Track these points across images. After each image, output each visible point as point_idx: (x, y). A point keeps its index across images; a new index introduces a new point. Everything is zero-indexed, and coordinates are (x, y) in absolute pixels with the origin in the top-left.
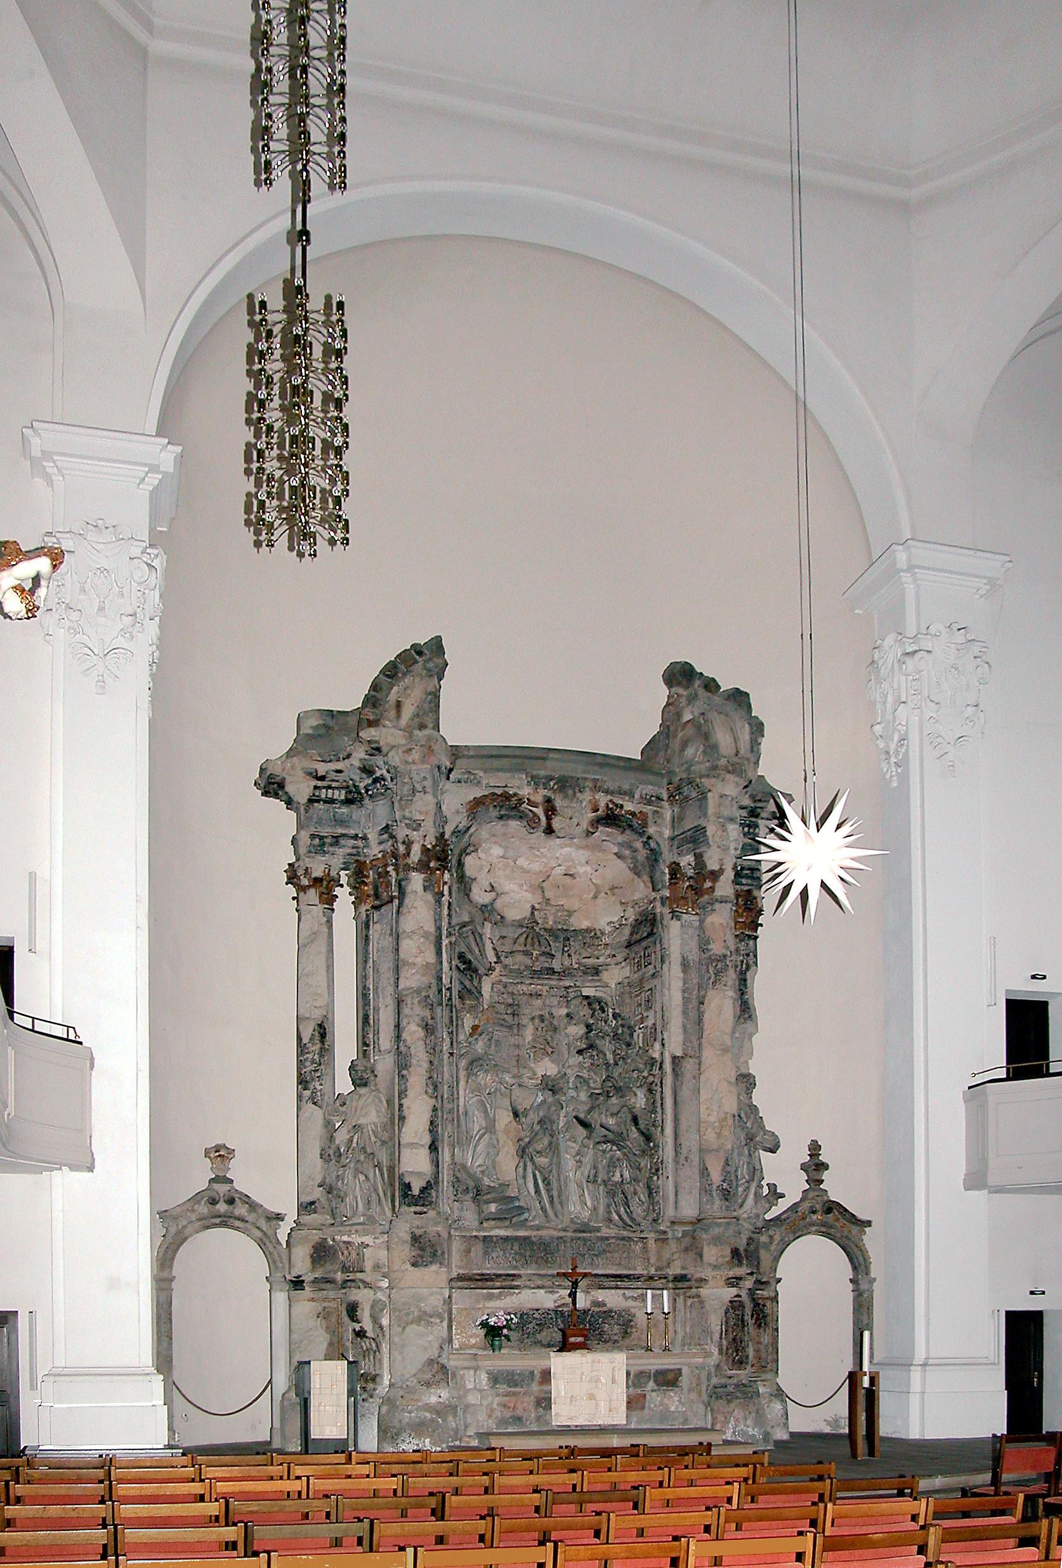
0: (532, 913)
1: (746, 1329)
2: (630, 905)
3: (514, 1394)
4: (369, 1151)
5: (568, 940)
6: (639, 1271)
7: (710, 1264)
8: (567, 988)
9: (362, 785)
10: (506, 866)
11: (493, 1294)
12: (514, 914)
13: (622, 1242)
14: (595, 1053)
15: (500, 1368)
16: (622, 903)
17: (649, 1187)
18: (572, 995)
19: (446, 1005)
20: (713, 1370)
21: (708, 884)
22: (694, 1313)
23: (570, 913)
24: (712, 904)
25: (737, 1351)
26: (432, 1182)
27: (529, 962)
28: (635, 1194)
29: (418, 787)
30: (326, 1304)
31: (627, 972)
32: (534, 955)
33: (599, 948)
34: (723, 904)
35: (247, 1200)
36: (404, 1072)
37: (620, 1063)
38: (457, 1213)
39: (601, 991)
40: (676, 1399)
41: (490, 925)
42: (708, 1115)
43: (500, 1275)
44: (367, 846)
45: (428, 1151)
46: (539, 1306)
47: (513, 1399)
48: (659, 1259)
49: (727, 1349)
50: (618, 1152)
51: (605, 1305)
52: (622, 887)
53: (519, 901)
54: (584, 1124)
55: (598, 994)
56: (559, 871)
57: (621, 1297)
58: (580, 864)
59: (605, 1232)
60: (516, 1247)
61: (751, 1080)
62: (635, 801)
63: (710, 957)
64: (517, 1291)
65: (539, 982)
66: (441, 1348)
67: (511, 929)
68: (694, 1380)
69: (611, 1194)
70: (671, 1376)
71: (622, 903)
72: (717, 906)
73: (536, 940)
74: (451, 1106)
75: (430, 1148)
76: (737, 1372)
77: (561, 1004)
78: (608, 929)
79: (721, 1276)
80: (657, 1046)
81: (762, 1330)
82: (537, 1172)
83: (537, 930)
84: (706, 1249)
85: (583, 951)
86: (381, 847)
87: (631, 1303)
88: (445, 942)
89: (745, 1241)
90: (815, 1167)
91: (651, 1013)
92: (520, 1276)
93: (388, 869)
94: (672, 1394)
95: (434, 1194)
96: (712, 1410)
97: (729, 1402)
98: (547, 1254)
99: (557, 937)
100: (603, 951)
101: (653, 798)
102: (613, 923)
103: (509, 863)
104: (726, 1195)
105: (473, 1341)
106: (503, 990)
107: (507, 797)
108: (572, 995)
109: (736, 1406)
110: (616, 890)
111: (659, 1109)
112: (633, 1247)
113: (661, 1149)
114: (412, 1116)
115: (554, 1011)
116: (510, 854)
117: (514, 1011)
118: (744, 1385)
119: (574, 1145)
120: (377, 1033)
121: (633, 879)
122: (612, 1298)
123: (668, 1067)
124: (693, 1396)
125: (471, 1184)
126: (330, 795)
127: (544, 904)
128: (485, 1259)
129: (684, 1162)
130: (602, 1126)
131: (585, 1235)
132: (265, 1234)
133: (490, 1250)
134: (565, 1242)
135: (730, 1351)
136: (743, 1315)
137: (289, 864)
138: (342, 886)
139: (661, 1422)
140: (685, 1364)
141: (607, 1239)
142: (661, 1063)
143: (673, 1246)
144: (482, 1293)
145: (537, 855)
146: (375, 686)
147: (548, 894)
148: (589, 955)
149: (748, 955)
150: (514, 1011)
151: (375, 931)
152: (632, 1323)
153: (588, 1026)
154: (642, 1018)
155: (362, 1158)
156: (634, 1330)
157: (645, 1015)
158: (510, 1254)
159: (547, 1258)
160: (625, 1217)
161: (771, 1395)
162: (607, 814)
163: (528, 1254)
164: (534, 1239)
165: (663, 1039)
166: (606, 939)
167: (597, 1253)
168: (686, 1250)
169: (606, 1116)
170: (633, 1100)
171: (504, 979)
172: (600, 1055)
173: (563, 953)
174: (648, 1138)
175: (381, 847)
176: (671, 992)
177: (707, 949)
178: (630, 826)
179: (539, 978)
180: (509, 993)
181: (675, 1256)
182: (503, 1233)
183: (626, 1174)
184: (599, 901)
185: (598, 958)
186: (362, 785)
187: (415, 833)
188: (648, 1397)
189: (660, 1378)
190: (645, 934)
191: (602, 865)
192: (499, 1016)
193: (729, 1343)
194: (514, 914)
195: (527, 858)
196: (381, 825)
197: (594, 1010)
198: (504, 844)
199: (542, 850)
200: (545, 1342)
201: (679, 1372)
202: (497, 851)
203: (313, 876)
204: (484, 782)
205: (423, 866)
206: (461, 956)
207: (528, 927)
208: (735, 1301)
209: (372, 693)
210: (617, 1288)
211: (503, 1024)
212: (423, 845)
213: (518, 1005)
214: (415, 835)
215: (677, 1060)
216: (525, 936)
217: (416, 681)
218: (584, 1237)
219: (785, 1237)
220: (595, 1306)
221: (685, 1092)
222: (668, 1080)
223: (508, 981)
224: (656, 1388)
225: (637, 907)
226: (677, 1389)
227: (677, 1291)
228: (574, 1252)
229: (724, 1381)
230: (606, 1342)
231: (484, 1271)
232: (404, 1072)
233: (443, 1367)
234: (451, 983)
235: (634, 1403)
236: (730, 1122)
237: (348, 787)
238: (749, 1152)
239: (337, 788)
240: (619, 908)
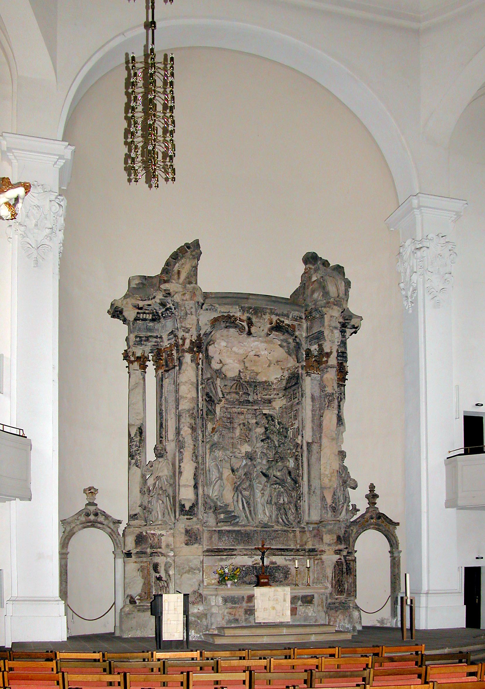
0: (239, 374)
2: (286, 369)
3: (235, 608)
4: (164, 489)
5: (256, 386)
6: (292, 547)
7: (326, 543)
8: (255, 410)
9: (160, 312)
10: (228, 351)
11: (223, 558)
12: (231, 374)
13: (284, 533)
14: (269, 441)
15: (228, 595)
16: (282, 369)
17: (296, 506)
18: (258, 413)
19: (201, 418)
20: (328, 595)
21: (325, 359)
22: (319, 568)
23: (257, 374)
24: (327, 369)
25: (340, 586)
26: (195, 504)
28: (290, 509)
29: (189, 312)
30: (142, 564)
31: (284, 402)
34: (332, 369)
35: (104, 514)
36: (182, 450)
37: (282, 446)
38: (205, 519)
40: (312, 610)
41: (220, 379)
42: (325, 471)
43: (227, 549)
44: (162, 341)
45: (193, 489)
46: (245, 564)
47: (234, 610)
48: (301, 541)
49: (335, 585)
50: (282, 489)
51: (276, 563)
52: (282, 361)
53: (233, 368)
54: (265, 475)
55: (271, 413)
56: (253, 353)
57: (284, 560)
58: (263, 351)
59: (276, 528)
60: (234, 536)
61: (344, 454)
62: (290, 319)
63: (326, 394)
64: (234, 557)
65: (243, 407)
66: (199, 585)
67: (229, 382)
68: (320, 601)
69: (279, 509)
70: (309, 599)
71: (282, 369)
72: (329, 369)
73: (241, 387)
74: (203, 467)
75: (194, 487)
76: (340, 596)
78: (275, 381)
79: (332, 549)
80: (300, 437)
81: (348, 576)
82: (243, 499)
83: (242, 382)
84: (325, 536)
86: (169, 342)
87: (288, 563)
88: (200, 387)
89: (343, 532)
90: (372, 496)
91: (297, 422)
92: (236, 549)
93: (173, 352)
94: (310, 607)
95: (196, 509)
96: (328, 615)
97: (336, 611)
99: (251, 385)
101: (298, 318)
102: (278, 378)
103: (228, 350)
104: (334, 509)
105: (213, 581)
106: (225, 410)
107: (229, 317)
108: (258, 413)
109: (340, 613)
110: (279, 363)
111: (301, 468)
113: (302, 488)
114: (185, 471)
115: (249, 421)
116: (230, 345)
118: (343, 603)
119: (260, 485)
120: (166, 432)
121: (288, 357)
122: (280, 560)
123: (305, 447)
124: (320, 608)
125: (212, 504)
126: (144, 317)
127: (245, 369)
129: (313, 494)
130: (274, 476)
131: (266, 529)
132: (112, 530)
134: (257, 533)
135: (337, 586)
136: (342, 569)
137: (125, 350)
138: (150, 361)
139: (305, 621)
140: (316, 593)
141: (277, 531)
142: (302, 446)
143: (308, 534)
144: (218, 558)
145: (242, 346)
146: (167, 264)
147: (247, 365)
149: (341, 394)
151: (166, 382)
152: (289, 572)
153: (266, 428)
154: (292, 424)
155: (161, 492)
156: (290, 576)
157: (293, 423)
158: (231, 538)
160: (285, 520)
161: (353, 608)
162: (277, 326)
163: (240, 538)
164: (242, 531)
165: (302, 434)
166: (274, 386)
168: (315, 536)
169: (276, 471)
170: (288, 464)
171: (226, 406)
172: (272, 442)
174: (296, 482)
175: (169, 342)
176: (306, 411)
177: (324, 390)
178: (287, 331)
179: (243, 405)
181: (309, 540)
182: (228, 528)
183: (286, 500)
184: (271, 368)
186: (160, 312)
187: (187, 334)
188: (298, 609)
189: (304, 599)
190: (294, 384)
191: (273, 350)
194: (231, 374)
195: (237, 347)
196: (169, 331)
197: (269, 421)
198: (226, 340)
199: (244, 343)
200: (248, 582)
201: (313, 597)
202: (224, 344)
203: (137, 356)
204: (219, 310)
205: (190, 350)
206: (207, 394)
207: (237, 381)
209: (166, 267)
210: (282, 555)
211: (225, 427)
212: (191, 340)
213: (233, 418)
214: (187, 335)
215: (309, 445)
216: (236, 385)
217: (187, 261)
218: (266, 530)
219: (358, 530)
220: (271, 564)
221: (313, 460)
222: (305, 454)
224: (302, 604)
225: (289, 371)
226: (312, 605)
227: (310, 557)
229: (333, 601)
230: (277, 581)
231: (219, 548)
232: (182, 450)
233: (200, 594)
234: (203, 407)
235: (294, 611)
236: (336, 474)
237: (153, 313)
238: (344, 489)
239: (148, 313)
240: (281, 371)
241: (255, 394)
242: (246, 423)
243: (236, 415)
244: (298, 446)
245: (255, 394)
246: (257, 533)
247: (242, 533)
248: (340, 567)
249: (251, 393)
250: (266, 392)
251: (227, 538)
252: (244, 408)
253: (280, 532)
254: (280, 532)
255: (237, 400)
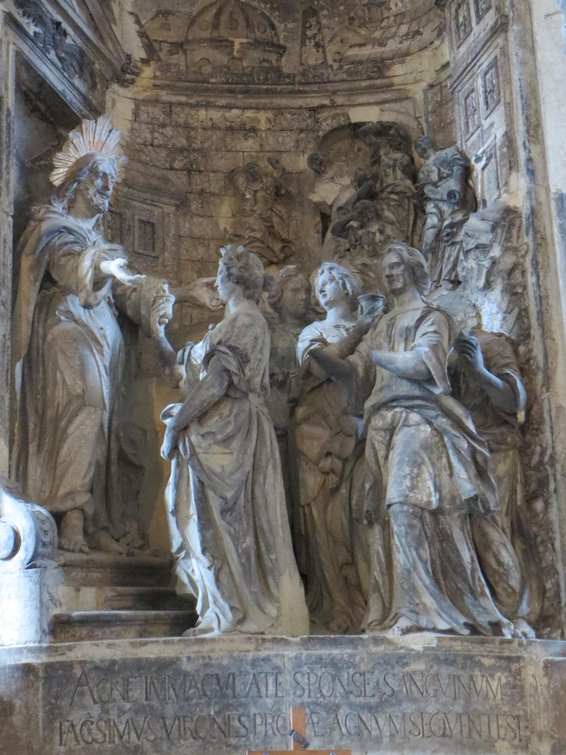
5: (315, 13)
8: (314, 110)
13: (445, 671)
18: (326, 125)
27: (222, 58)
32: (237, 46)
33: (384, 23)
39: (391, 110)
55: (388, 117)
60: (137, 693)
65: (251, 101)
77: (302, 145)
85: (350, 35)
98: (227, 707)
100: (393, 30)
106: (162, 118)
112: (481, 683)
113: (547, 428)
117: (191, 163)
128: (52, 730)
133: (64, 703)
134: (278, 671)
148: (360, 41)
150: (191, 163)
158: (122, 712)
159: (227, 721)
163: (170, 710)
164: (187, 666)
167: (373, 701)
171: (165, 96)
173: (303, 43)
179: (246, 93)
180: (177, 125)
185: (382, 44)
192: (153, 170)
216: (214, 10)
223: (174, 99)
228: (306, 699)
241: (310, 44)
242: (263, 164)
243: (216, 136)
244: (511, 224)
245: (310, 44)
246: (278, 671)
247: (186, 674)
249: (288, 45)
250: (363, 32)
251: (96, 711)
252: (258, 108)
253: (420, 666)
254: (420, 666)
255: (217, 69)
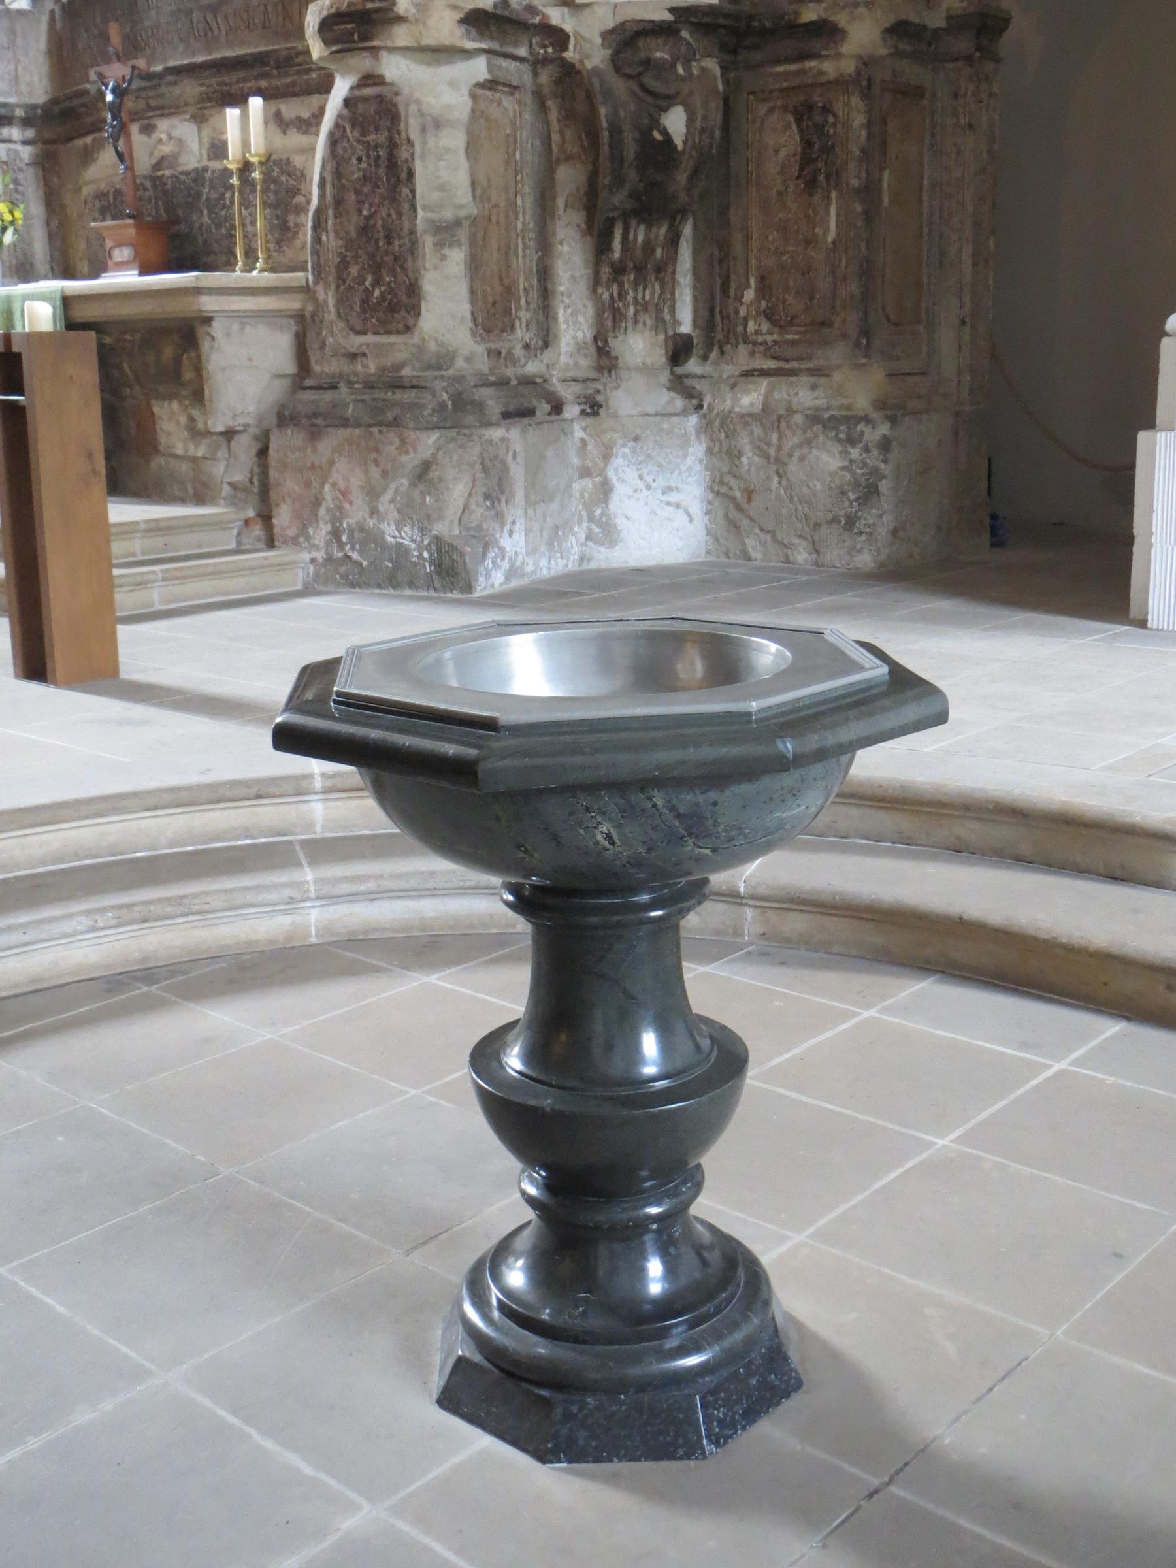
1: (406, 191)
25: (377, 268)
49: (343, 265)
97: (315, 434)
135: (354, 270)
136: (393, 146)
193: (349, 244)
208: (365, 99)
248: (372, 137)
